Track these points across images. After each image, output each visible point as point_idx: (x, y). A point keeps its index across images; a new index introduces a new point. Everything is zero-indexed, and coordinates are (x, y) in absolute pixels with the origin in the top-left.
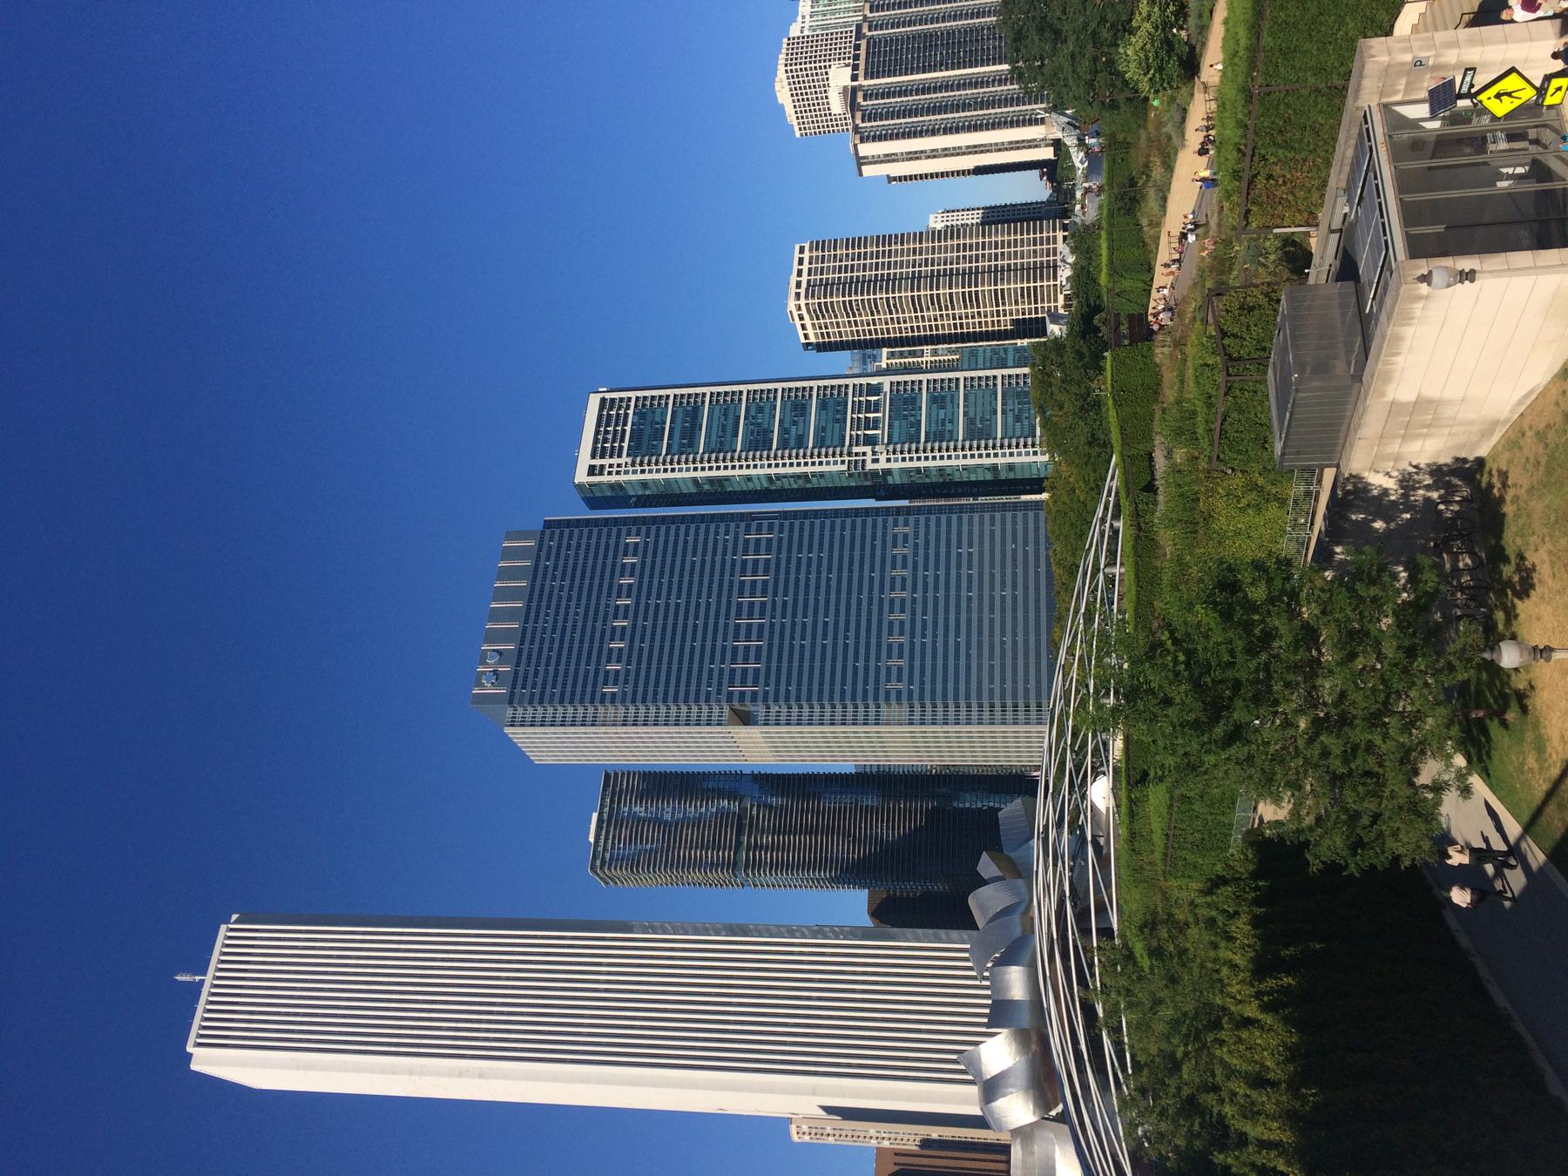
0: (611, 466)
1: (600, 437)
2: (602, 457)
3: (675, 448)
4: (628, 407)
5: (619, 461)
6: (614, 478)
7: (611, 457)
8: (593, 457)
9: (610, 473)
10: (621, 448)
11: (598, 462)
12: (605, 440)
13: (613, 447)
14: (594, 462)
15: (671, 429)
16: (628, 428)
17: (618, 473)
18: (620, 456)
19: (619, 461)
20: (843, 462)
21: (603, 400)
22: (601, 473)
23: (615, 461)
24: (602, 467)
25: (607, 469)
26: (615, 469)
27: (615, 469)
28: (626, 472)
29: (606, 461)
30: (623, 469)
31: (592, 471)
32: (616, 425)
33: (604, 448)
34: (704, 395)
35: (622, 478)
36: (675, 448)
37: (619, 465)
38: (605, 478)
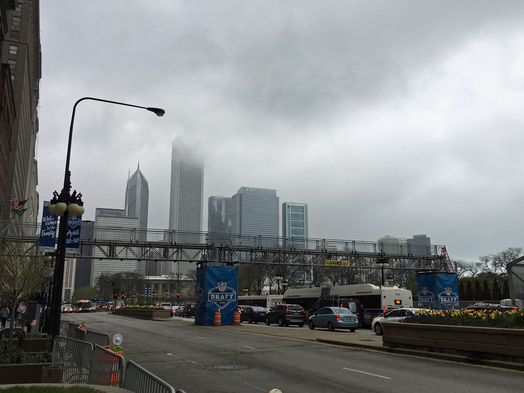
0: (289, 210)
4: (302, 212)
5: (290, 211)
7: (291, 210)
8: (291, 206)
9: (288, 210)
14: (290, 206)
15: (297, 222)
19: (290, 211)
21: (304, 207)
22: (288, 208)
23: (290, 211)
24: (289, 208)
25: (289, 209)
30: (289, 212)
34: (304, 228)
36: (293, 222)
37: (289, 211)
38: (287, 209)
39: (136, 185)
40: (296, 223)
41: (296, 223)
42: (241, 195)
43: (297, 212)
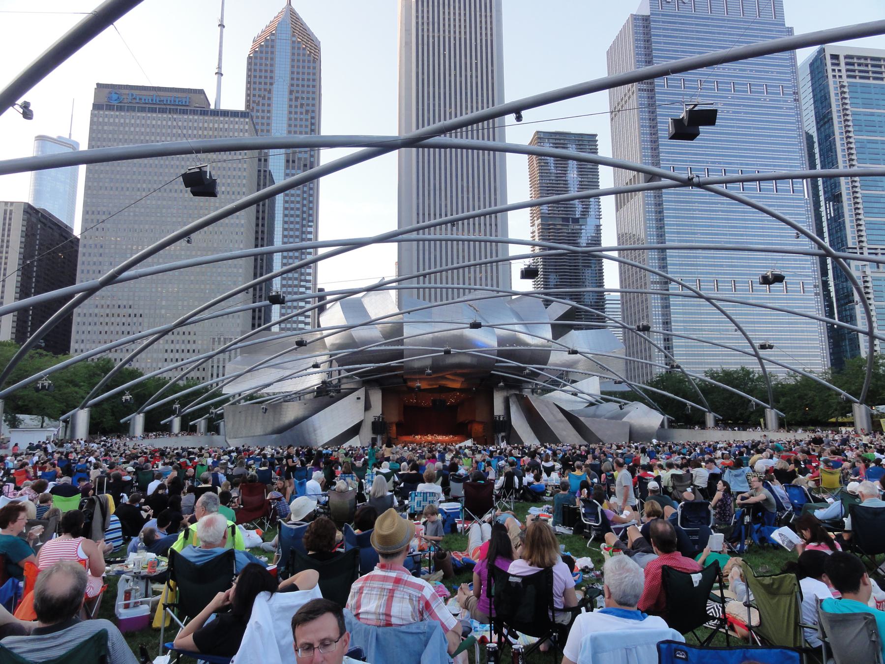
0: (840, 71)
1: (862, 61)
2: (847, 64)
3: (858, 117)
5: (844, 77)
6: (830, 74)
7: (847, 70)
8: (846, 57)
9: (834, 70)
10: (855, 77)
11: (842, 61)
12: (859, 65)
13: (854, 71)
16: (871, 81)
17: (834, 76)
18: (848, 76)
19: (844, 77)
20: (854, 243)
22: (833, 64)
23: (844, 73)
24: (838, 65)
25: (837, 68)
26: (837, 74)
27: (837, 74)
28: (835, 83)
29: (843, 67)
31: (835, 57)
32: (874, 72)
33: (853, 64)
35: (831, 80)
36: (858, 117)
37: (840, 77)
38: (829, 67)
39: (273, 40)
40: (872, 118)
41: (872, 118)
42: (646, 19)
43: (868, 78)
